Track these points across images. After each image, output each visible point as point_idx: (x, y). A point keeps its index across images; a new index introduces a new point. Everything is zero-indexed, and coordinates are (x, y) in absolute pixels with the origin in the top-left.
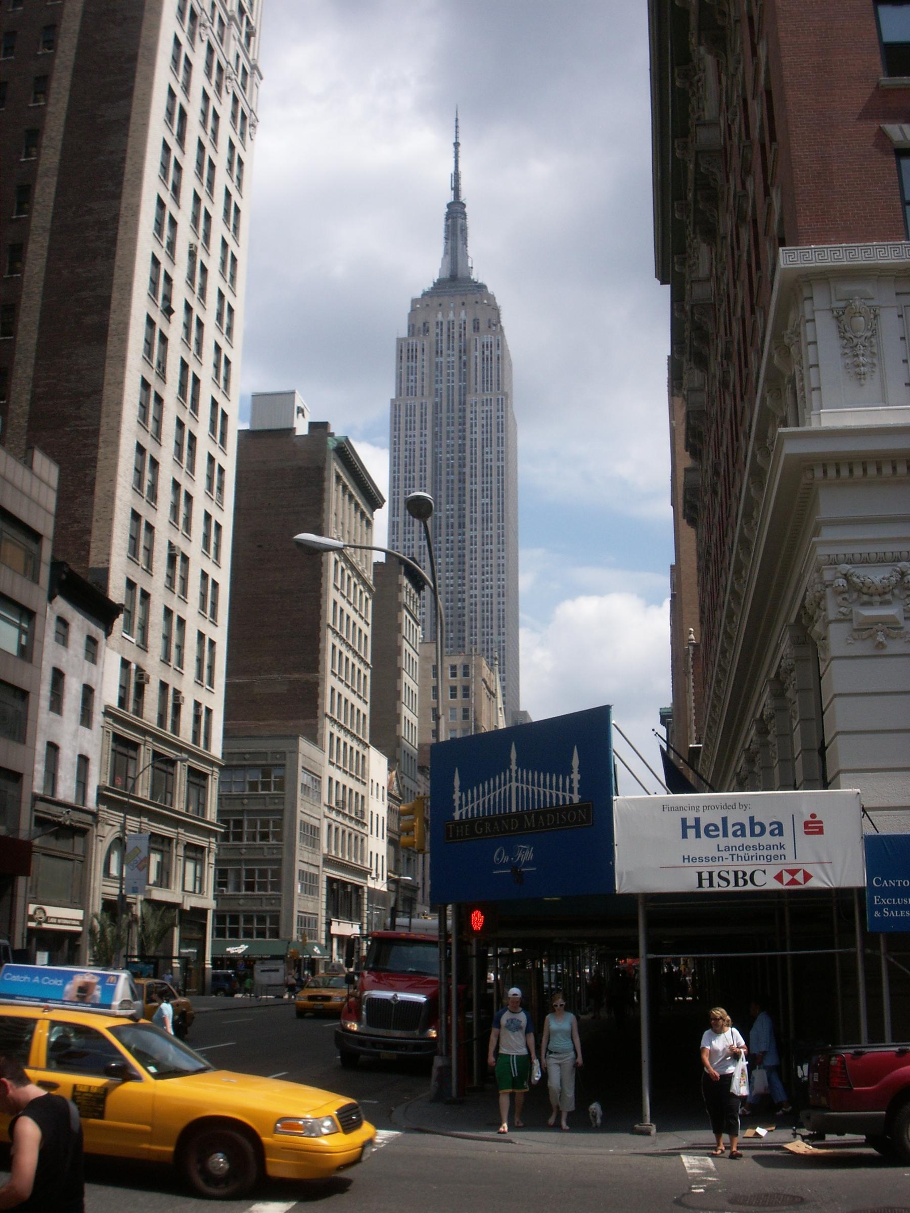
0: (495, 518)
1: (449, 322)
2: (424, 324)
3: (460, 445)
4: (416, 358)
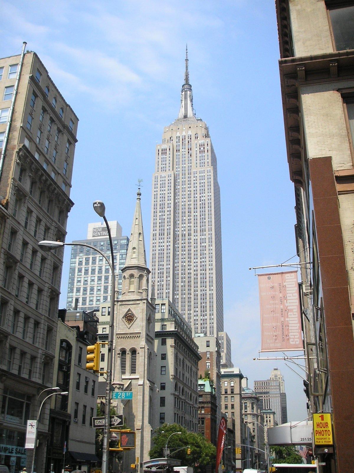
0: (207, 229)
1: (183, 136)
2: (170, 138)
3: (189, 194)
4: (166, 153)
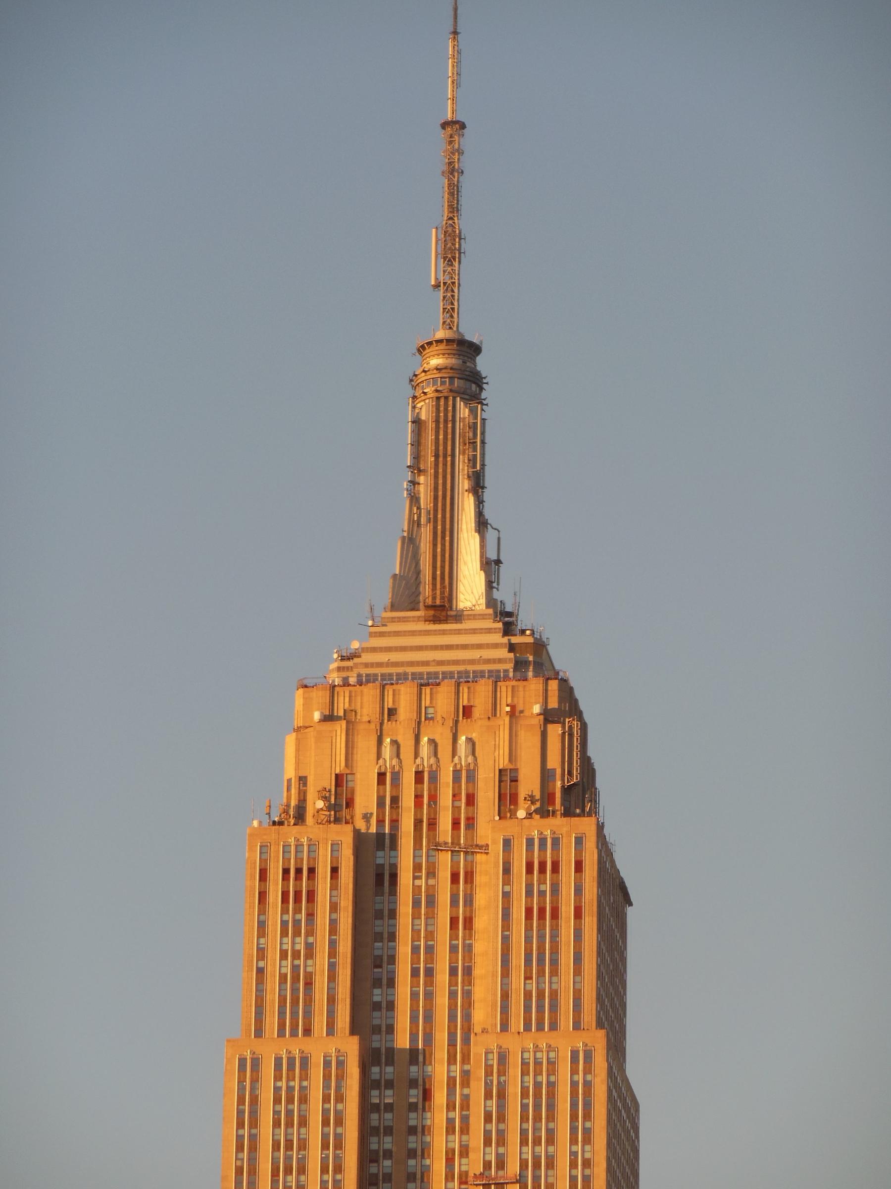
2: (339, 779)
